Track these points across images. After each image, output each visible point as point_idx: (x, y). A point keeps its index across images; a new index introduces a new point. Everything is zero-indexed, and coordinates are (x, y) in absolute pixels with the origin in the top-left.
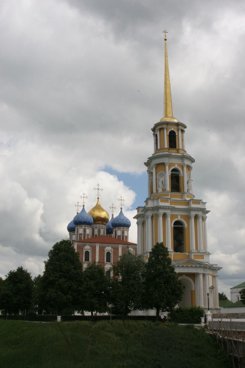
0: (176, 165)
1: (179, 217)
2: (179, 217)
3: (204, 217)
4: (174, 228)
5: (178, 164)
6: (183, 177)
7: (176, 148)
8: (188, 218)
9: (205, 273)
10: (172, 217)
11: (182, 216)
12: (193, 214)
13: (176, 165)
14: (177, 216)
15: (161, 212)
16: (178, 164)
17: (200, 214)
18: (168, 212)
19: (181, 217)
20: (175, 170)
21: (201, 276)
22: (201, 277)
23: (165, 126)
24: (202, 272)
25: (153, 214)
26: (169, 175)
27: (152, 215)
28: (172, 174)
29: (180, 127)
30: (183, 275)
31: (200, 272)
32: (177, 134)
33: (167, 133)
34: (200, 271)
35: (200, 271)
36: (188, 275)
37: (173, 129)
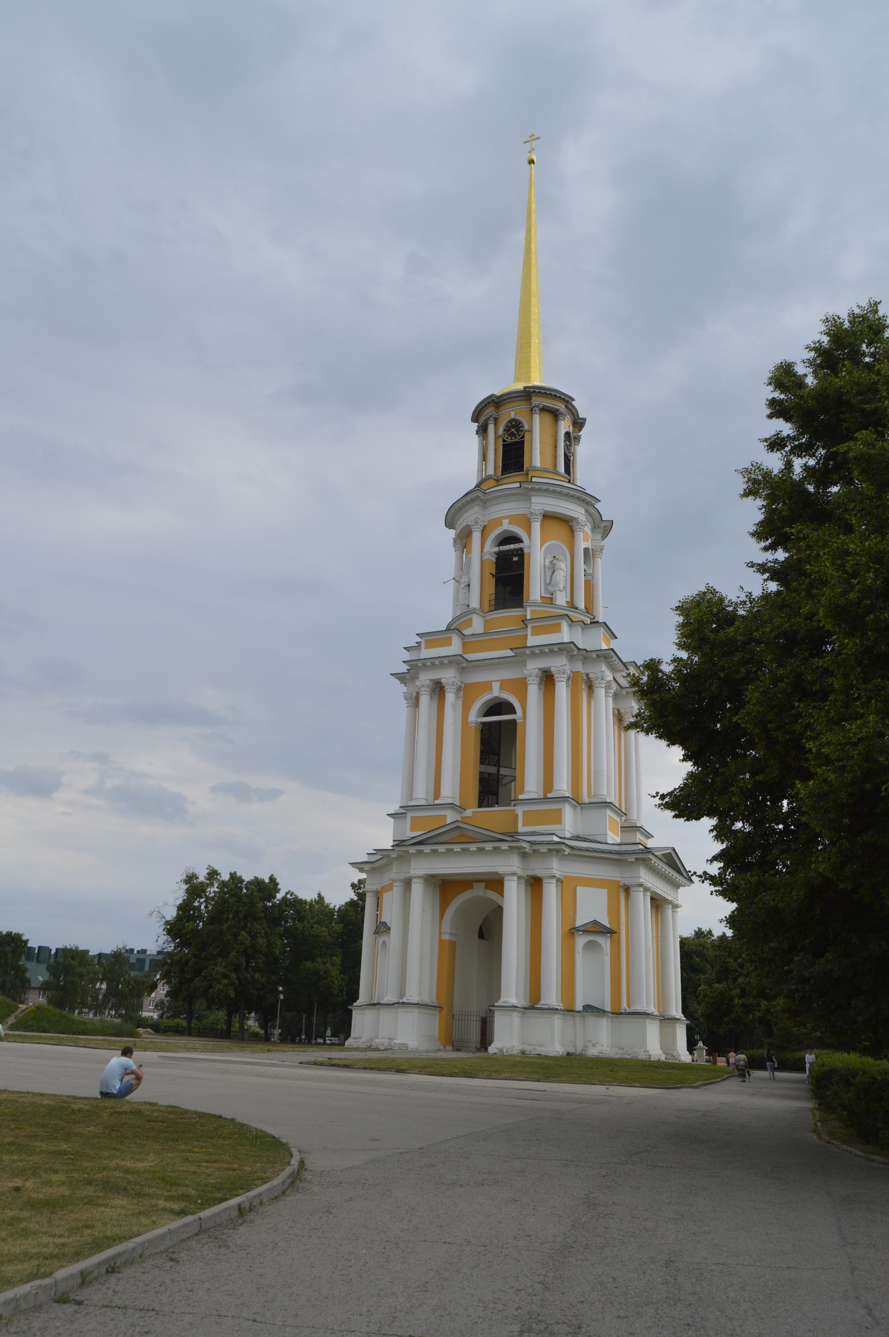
0: (505, 522)
1: (496, 686)
2: (496, 686)
3: (591, 676)
5: (513, 519)
6: (529, 554)
8: (520, 686)
9: (539, 873)
10: (467, 692)
12: (533, 667)
13: (505, 522)
14: (488, 686)
15: (425, 678)
16: (513, 519)
17: (559, 665)
18: (448, 676)
19: (501, 688)
20: (510, 539)
23: (490, 410)
26: (482, 563)
27: (415, 694)
30: (474, 884)
31: (501, 870)
32: (526, 427)
33: (496, 432)
34: (509, 866)
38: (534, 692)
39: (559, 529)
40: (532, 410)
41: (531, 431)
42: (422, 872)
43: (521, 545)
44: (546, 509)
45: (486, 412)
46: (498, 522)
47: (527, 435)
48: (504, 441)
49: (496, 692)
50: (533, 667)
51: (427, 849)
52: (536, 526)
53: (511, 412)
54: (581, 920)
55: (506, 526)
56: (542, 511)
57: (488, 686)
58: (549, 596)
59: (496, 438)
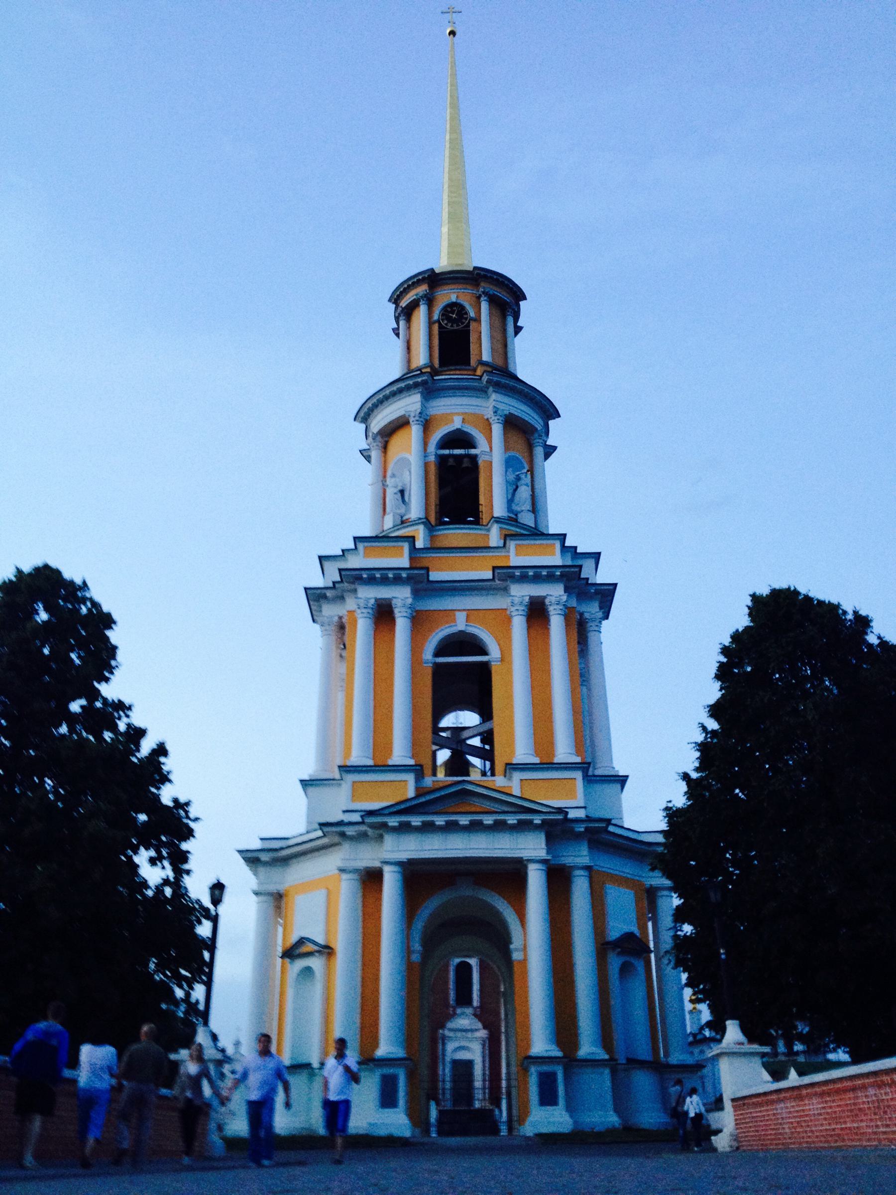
1: (461, 617)
2: (461, 617)
4: (437, 667)
7: (469, 364)
11: (471, 614)
14: (449, 614)
20: (459, 439)
21: (536, 880)
22: (536, 880)
23: (422, 289)
24: (542, 853)
25: (340, 618)
26: (426, 465)
27: (336, 619)
28: (442, 461)
29: (484, 286)
31: (525, 855)
32: (472, 314)
35: (531, 847)
37: (453, 298)
38: (519, 624)
39: (518, 441)
40: (479, 297)
41: (478, 320)
42: (404, 856)
43: (473, 451)
44: (512, 412)
45: (422, 289)
47: (473, 325)
48: (440, 326)
49: (460, 624)
50: (522, 592)
51: (416, 821)
52: (497, 430)
53: (448, 295)
54: (614, 934)
56: (507, 412)
57: (449, 614)
58: (513, 516)
59: (431, 323)
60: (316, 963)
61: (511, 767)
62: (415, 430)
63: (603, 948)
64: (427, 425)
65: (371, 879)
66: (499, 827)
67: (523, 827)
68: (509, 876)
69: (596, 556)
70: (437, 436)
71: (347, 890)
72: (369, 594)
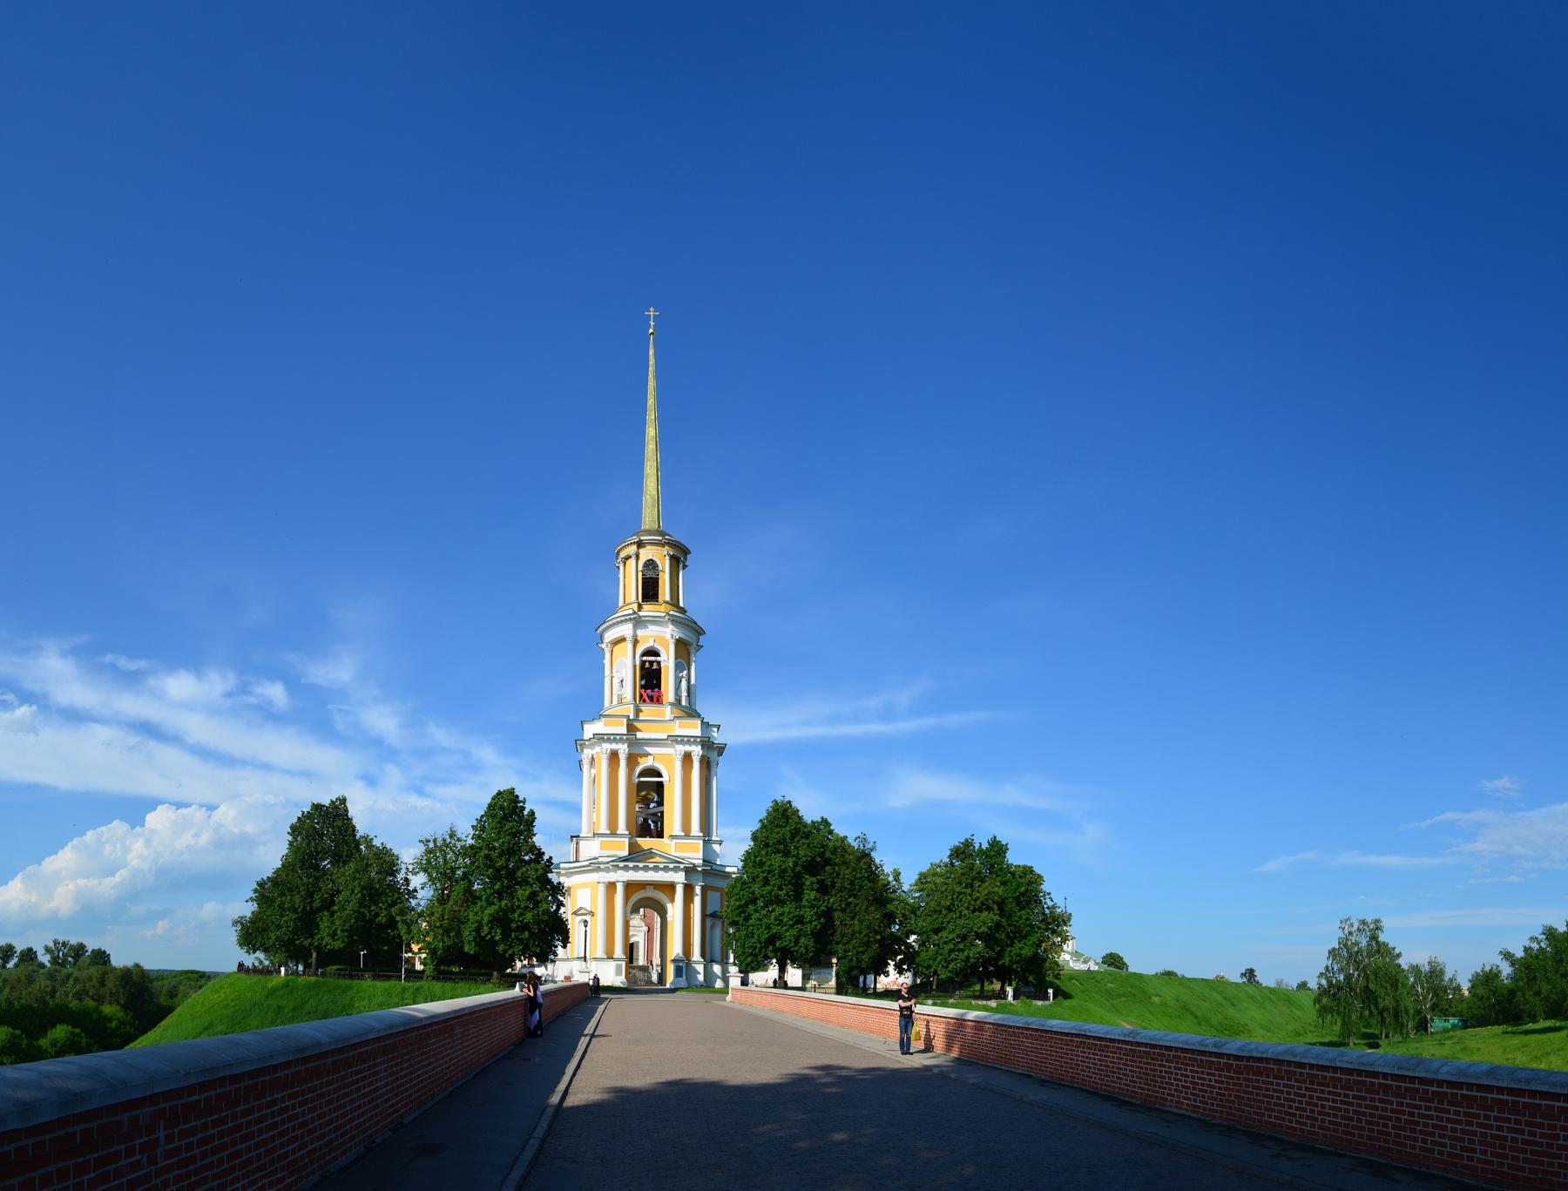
10: (632, 760)
20: (652, 652)
21: (679, 890)
28: (643, 663)
36: (658, 886)
38: (678, 765)
46: (648, 637)
53: (647, 554)
55: (650, 644)
60: (587, 918)
61: (673, 837)
62: (629, 645)
63: (704, 916)
64: (636, 642)
65: (611, 886)
66: (666, 869)
67: (676, 869)
68: (669, 888)
69: (718, 727)
70: (639, 651)
71: (601, 890)
72: (608, 747)
